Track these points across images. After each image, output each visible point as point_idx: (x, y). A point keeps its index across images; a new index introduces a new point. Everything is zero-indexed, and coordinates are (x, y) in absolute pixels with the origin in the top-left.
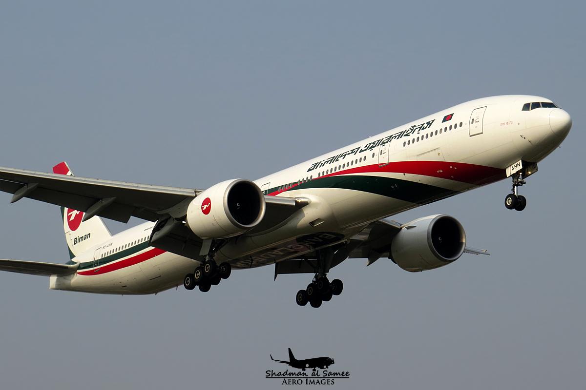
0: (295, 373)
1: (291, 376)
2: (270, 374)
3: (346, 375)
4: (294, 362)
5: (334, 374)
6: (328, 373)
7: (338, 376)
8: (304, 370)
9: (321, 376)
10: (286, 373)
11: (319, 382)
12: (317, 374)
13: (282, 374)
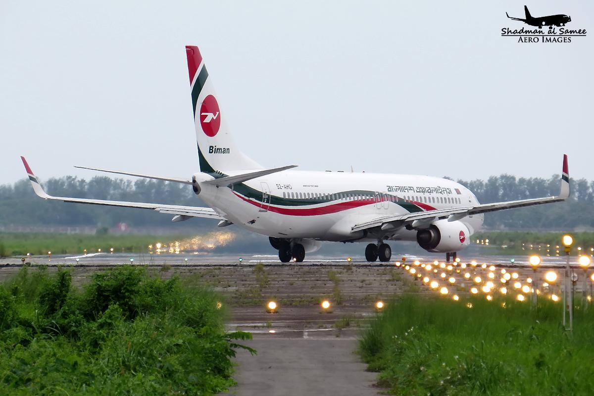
0: (531, 31)
1: (528, 34)
2: (506, 32)
3: (583, 33)
4: (530, 20)
5: (571, 32)
6: (564, 31)
7: (575, 34)
8: (540, 27)
9: (558, 34)
10: (522, 30)
11: (555, 40)
12: (554, 32)
13: (518, 32)
